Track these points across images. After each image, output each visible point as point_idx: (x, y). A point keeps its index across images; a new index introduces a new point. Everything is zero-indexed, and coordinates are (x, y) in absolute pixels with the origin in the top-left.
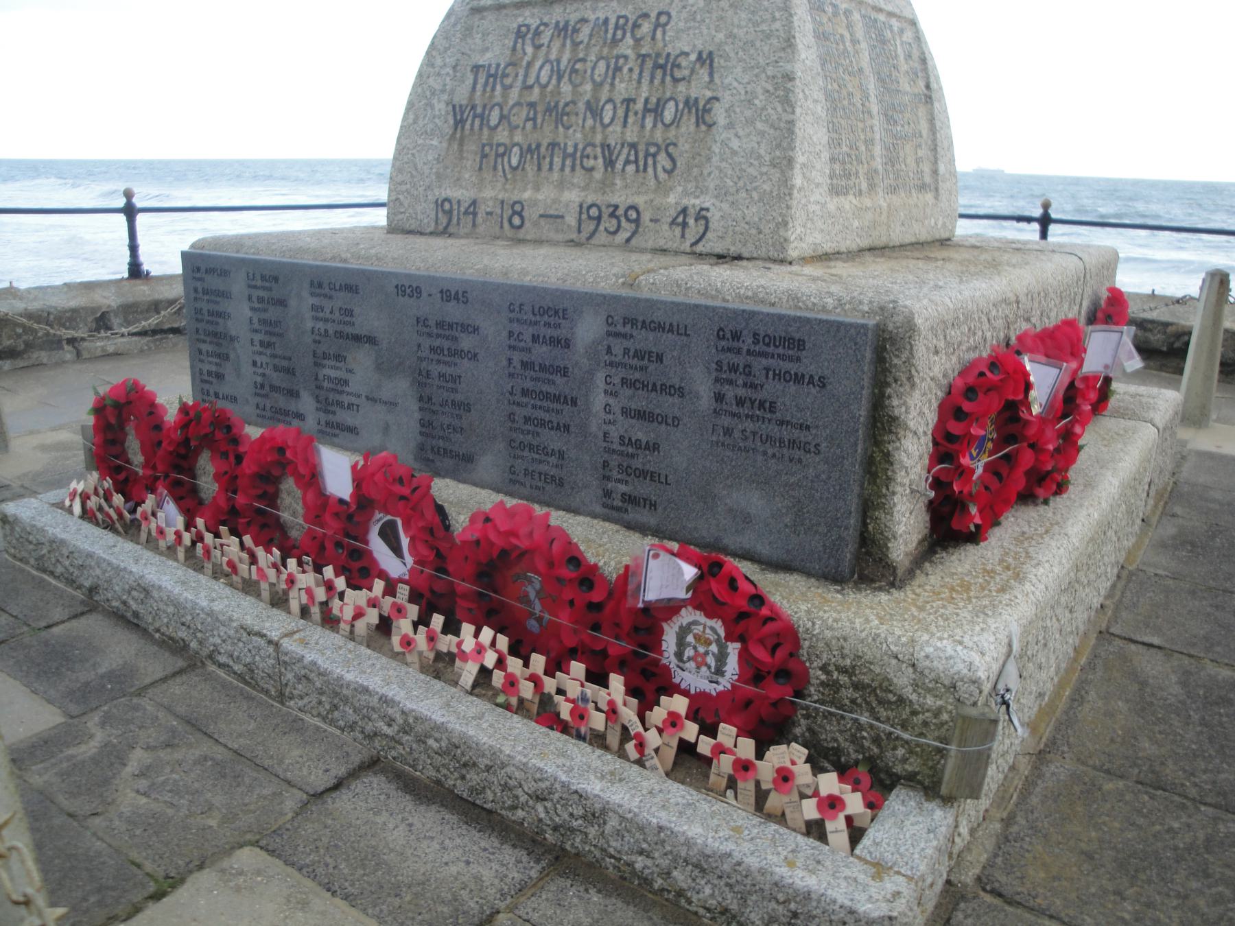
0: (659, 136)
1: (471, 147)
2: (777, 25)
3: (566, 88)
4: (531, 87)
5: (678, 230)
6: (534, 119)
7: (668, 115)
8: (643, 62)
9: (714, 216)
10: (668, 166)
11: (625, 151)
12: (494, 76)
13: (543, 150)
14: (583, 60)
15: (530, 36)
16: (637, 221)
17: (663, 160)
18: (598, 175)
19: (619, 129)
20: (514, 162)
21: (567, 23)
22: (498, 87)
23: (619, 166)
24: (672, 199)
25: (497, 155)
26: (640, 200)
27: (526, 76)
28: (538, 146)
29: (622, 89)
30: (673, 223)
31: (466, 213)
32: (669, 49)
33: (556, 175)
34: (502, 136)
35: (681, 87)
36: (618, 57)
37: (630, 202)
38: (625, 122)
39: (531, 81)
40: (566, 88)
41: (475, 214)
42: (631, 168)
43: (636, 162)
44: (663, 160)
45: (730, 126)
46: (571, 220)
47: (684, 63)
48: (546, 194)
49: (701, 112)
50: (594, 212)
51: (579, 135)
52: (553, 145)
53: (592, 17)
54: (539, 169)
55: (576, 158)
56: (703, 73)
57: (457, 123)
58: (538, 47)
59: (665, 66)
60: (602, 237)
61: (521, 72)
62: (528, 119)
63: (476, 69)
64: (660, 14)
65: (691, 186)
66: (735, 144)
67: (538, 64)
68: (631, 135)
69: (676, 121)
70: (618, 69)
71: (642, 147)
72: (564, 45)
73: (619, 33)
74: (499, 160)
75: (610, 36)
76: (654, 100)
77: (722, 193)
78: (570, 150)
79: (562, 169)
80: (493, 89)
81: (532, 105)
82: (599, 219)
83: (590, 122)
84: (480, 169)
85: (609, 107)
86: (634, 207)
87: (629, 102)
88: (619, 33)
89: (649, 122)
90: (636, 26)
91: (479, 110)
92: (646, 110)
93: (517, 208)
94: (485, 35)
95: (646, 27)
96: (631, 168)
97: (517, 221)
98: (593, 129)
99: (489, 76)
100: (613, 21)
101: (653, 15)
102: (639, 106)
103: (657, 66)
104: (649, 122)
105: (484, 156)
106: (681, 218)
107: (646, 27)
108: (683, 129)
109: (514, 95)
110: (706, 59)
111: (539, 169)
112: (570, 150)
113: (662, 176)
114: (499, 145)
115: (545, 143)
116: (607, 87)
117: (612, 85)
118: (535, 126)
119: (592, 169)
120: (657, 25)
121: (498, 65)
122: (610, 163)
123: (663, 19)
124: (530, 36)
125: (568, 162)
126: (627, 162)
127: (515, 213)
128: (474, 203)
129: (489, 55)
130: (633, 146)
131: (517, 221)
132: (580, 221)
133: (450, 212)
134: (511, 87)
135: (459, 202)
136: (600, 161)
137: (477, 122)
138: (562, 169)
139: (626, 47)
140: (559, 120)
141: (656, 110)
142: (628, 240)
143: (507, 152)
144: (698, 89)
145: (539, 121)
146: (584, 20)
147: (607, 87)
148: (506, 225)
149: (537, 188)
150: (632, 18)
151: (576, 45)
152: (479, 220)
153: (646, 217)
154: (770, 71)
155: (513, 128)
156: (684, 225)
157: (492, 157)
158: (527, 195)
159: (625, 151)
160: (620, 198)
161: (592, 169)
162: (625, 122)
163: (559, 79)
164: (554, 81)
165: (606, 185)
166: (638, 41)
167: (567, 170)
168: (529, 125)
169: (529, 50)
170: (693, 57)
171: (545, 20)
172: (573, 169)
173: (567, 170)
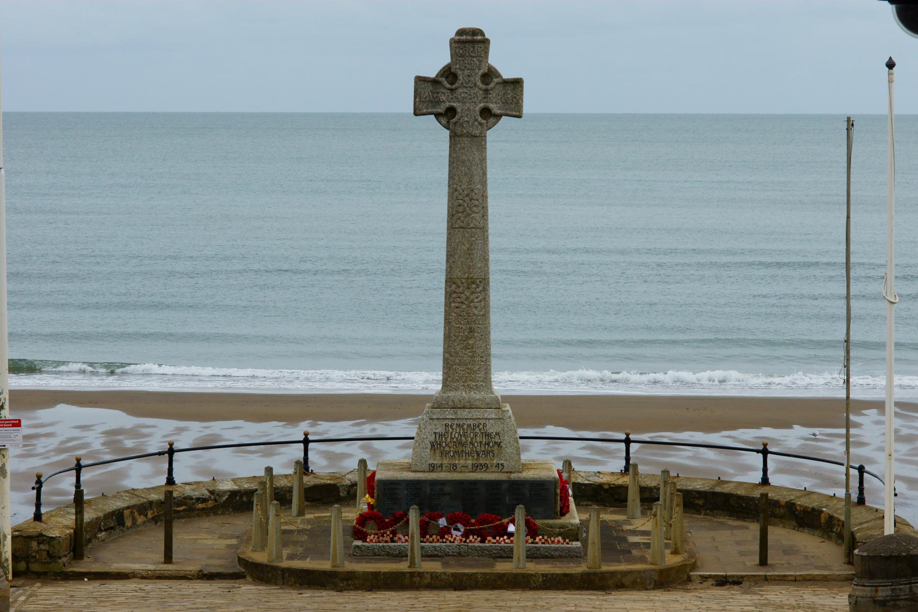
0: (489, 449)
1: (438, 452)
2: (513, 428)
3: (463, 439)
4: (453, 438)
5: (497, 468)
6: (456, 445)
7: (491, 445)
8: (482, 435)
9: (505, 465)
10: (492, 455)
11: (482, 452)
12: (441, 435)
13: (460, 452)
14: (467, 433)
15: (449, 426)
16: (487, 467)
17: (491, 454)
18: (475, 457)
19: (479, 448)
20: (452, 455)
21: (459, 424)
22: (443, 438)
23: (481, 455)
24: (495, 462)
25: (446, 453)
26: (487, 462)
27: (451, 436)
28: (458, 451)
29: (478, 439)
30: (496, 466)
31: (439, 466)
32: (488, 431)
33: (464, 458)
34: (447, 449)
35: (493, 439)
36: (476, 433)
37: (485, 462)
38: (481, 447)
39: (453, 437)
40: (463, 439)
41: (442, 467)
42: (483, 456)
43: (485, 454)
44: (491, 454)
45: (507, 447)
46: (470, 467)
47: (493, 435)
48: (462, 462)
49: (499, 445)
50: (476, 465)
51: (469, 449)
52: (462, 451)
53: (466, 423)
54: (459, 456)
55: (469, 454)
56: (498, 437)
57: (432, 446)
58: (453, 429)
59: (488, 435)
60: (478, 470)
61: (450, 435)
62: (454, 445)
63: (435, 433)
64: (484, 424)
65: (499, 459)
66: (508, 451)
67: (454, 433)
68: (483, 449)
69: (493, 446)
70: (476, 435)
71: (486, 452)
72: (460, 429)
73: (475, 427)
74: (447, 455)
75: (472, 428)
76: (487, 442)
77: (506, 460)
78: (467, 452)
79: (466, 456)
80: (442, 438)
81: (455, 442)
82: (477, 467)
83: (471, 446)
84: (441, 456)
85: (476, 443)
86: (486, 464)
87: (481, 442)
88: (475, 427)
89: (487, 446)
90: (478, 426)
91: (439, 443)
92: (485, 444)
93: (455, 465)
94: (435, 425)
95: (481, 427)
96: (483, 456)
97: (455, 468)
98: (473, 448)
99: (439, 435)
100: (472, 425)
101: (482, 424)
102: (484, 443)
103: (486, 435)
104: (487, 446)
105: (442, 453)
106: (498, 465)
107: (481, 427)
108: (495, 448)
109: (449, 440)
110: (497, 434)
111: (459, 456)
112: (467, 452)
113: (492, 457)
114: (446, 451)
115: (460, 451)
116: (474, 439)
117: (476, 438)
118: (456, 447)
119: (474, 456)
120: (484, 426)
121: (442, 433)
122: (478, 455)
123: (485, 425)
124: (449, 426)
125: (467, 455)
126: (482, 454)
127: (454, 466)
128: (442, 464)
129: (438, 430)
130: (483, 451)
131: (455, 468)
132: (472, 467)
133: (434, 466)
134: (447, 438)
135: (437, 464)
136: (476, 454)
137: (439, 446)
138: (466, 456)
139: (477, 430)
140: (463, 446)
141: (488, 444)
142: (485, 470)
143: (449, 452)
144: (497, 440)
145: (457, 446)
146: (464, 424)
147: (474, 439)
148: (452, 469)
149: (459, 460)
150: (477, 424)
151: (463, 429)
152: (443, 468)
153: (489, 466)
154: (513, 437)
155: (450, 447)
156: (498, 467)
157: (444, 454)
158: (457, 462)
159: (482, 452)
160: (482, 461)
161: (474, 456)
162: (481, 447)
163: (461, 437)
164: (460, 437)
165: (477, 460)
166: (480, 429)
167: (467, 456)
168: (455, 447)
169: (450, 430)
170: (494, 433)
171: (453, 423)
172: (469, 456)
173: (467, 456)
